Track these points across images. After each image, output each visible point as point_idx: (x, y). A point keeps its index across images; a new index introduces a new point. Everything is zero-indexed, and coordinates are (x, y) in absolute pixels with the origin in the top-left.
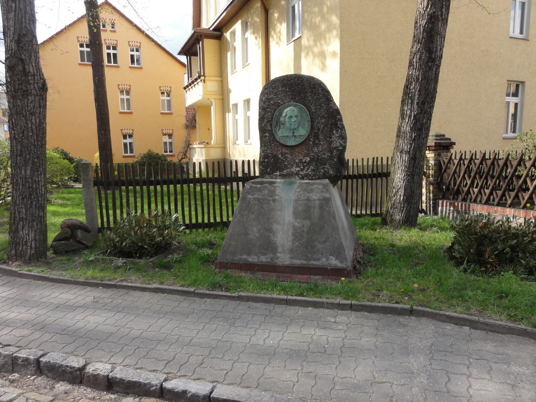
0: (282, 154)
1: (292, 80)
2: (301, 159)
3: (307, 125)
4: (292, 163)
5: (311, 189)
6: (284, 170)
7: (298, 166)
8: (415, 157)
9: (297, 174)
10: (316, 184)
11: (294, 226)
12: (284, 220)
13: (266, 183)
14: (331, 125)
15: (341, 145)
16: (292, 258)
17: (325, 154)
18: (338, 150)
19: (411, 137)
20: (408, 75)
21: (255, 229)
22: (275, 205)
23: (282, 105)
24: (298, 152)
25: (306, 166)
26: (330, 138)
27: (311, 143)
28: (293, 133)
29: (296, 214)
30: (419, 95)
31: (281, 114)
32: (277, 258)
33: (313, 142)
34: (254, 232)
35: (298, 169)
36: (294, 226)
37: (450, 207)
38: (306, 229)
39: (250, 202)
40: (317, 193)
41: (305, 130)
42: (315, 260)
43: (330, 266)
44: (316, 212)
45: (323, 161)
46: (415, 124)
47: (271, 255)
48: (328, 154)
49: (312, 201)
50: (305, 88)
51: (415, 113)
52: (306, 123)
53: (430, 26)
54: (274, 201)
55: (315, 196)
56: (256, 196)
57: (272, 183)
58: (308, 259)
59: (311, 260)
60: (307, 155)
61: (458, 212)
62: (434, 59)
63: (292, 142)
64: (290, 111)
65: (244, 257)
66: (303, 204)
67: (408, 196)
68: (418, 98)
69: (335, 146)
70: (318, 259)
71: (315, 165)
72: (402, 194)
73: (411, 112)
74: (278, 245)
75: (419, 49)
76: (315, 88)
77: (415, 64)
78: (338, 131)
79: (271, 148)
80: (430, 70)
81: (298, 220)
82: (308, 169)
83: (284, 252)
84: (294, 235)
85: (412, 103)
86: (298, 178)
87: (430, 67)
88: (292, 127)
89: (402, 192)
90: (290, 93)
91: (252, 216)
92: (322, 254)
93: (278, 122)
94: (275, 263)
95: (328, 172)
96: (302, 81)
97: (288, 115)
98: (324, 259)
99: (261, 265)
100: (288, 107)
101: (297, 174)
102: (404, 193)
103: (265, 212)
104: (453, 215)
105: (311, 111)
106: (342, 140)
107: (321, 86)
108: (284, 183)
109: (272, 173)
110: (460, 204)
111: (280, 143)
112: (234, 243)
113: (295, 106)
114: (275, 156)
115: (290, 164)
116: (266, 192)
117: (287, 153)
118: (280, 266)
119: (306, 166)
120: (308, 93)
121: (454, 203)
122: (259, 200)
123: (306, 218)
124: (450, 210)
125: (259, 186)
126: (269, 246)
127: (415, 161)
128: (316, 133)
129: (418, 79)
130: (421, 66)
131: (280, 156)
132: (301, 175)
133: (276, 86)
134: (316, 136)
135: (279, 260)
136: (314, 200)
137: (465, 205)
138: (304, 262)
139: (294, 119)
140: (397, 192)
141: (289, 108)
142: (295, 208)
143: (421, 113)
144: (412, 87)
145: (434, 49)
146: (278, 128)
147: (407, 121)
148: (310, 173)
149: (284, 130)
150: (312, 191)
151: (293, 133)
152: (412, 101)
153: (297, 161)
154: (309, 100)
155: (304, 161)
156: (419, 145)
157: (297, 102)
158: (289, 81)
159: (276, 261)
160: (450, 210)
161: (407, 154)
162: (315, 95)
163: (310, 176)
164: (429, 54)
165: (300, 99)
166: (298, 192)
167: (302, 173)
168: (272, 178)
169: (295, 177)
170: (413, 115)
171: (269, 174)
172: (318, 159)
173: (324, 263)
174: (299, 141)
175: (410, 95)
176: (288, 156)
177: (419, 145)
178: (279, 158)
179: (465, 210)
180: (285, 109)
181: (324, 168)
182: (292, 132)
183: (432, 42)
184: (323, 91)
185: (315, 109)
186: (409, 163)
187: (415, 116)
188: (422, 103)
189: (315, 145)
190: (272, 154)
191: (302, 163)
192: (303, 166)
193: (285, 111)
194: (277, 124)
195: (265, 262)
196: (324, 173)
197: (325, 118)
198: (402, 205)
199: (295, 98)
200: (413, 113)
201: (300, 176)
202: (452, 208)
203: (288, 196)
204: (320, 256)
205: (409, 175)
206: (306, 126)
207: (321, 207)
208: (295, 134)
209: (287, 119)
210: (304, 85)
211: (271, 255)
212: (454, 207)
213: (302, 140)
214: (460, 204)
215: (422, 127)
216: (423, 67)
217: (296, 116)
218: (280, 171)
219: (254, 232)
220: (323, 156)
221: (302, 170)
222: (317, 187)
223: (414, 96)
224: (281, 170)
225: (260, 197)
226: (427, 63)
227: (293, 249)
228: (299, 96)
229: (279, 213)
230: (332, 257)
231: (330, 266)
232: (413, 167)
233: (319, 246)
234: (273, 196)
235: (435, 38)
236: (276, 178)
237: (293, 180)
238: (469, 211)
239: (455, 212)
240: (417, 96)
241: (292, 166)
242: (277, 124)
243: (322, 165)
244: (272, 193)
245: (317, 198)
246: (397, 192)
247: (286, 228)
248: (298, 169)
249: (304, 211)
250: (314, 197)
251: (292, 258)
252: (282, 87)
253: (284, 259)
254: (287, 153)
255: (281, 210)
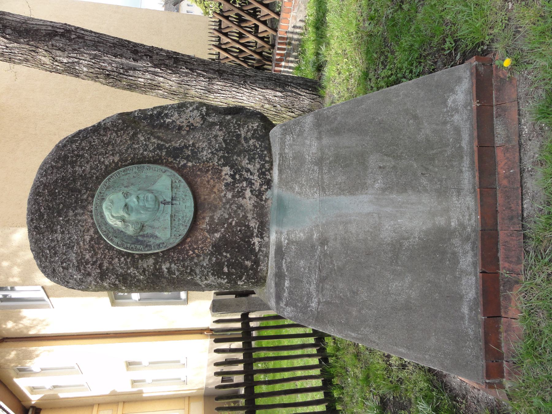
0: (212, 231)
1: (39, 210)
2: (227, 185)
3: (150, 171)
4: (234, 207)
5: (294, 158)
6: (248, 227)
7: (240, 194)
8: (218, 71)
9: (259, 195)
10: (282, 148)
11: (384, 190)
12: (369, 214)
13: (279, 267)
14: (154, 127)
15: (197, 108)
16: (459, 191)
17: (216, 136)
18: (208, 114)
19: (187, 74)
20: (88, 76)
21: (395, 285)
22: (335, 239)
23: (96, 232)
24: (209, 194)
25: (241, 175)
26: (180, 128)
27: (190, 164)
28: (165, 203)
29: (355, 187)
30: (122, 56)
31: (117, 233)
32: (463, 226)
33: (189, 161)
34: (402, 287)
35: (248, 193)
36: (384, 190)
37: (281, 66)
38: (390, 163)
39: (327, 303)
40: (304, 144)
41: (159, 177)
42: (458, 139)
43: (470, 104)
44: (349, 142)
45: (231, 140)
46: (167, 66)
47: (456, 241)
48: (216, 130)
49: (323, 153)
50: (63, 179)
51: (150, 65)
52: (143, 175)
53: (9, 31)
54: (324, 242)
55: (311, 147)
56: (313, 287)
57: (280, 252)
58: (459, 154)
59: (460, 147)
60: (217, 172)
61: (288, 55)
62: (66, 30)
63: (187, 207)
64: (114, 211)
65: (465, 310)
66: (329, 172)
67: (275, 84)
68: (126, 58)
69: (198, 119)
70: (457, 130)
71: (239, 155)
72: (273, 92)
73: (148, 72)
74: (429, 225)
75: (46, 51)
76: (66, 157)
77: (71, 60)
78: (166, 115)
79: (198, 256)
80: (83, 38)
81: (369, 182)
82: (248, 170)
83: (447, 210)
84: (403, 189)
85: (135, 69)
86: (269, 193)
87: (79, 37)
88: (150, 204)
89: (270, 94)
90: (71, 213)
91: (363, 295)
92: (445, 123)
93: (136, 240)
94: (474, 231)
95: (255, 130)
96: (45, 186)
97: (122, 213)
98: (456, 117)
99: (483, 266)
100: (103, 217)
101: (259, 195)
102: (272, 89)
103: (351, 262)
104: (292, 62)
105: (117, 164)
106: (187, 108)
107: (65, 146)
108: (280, 223)
109: (256, 255)
110: (278, 52)
111: (188, 235)
112: (433, 340)
113: (103, 199)
114: (217, 248)
115: (235, 212)
116: (302, 263)
117: (212, 218)
118: (482, 217)
119: (241, 175)
120: (75, 172)
121: (277, 60)
122: (322, 280)
123: (363, 163)
124: (285, 67)
125: (287, 283)
126: (435, 248)
127: (224, 72)
128: (169, 153)
129: (95, 57)
130: (75, 50)
131: (217, 235)
132: (261, 185)
133: (49, 248)
134: (176, 153)
135: (466, 222)
136: (321, 149)
137: (279, 43)
138: (466, 162)
139: (133, 201)
140: (269, 102)
141: (107, 214)
142: (342, 191)
143: (151, 57)
144: (109, 68)
145: (50, 28)
146: (152, 240)
147: (161, 79)
148: (258, 166)
149: (156, 224)
150: (299, 157)
151: (165, 203)
152: (130, 69)
153: (229, 195)
154: (91, 168)
155: (230, 180)
156: (199, 65)
157: (93, 197)
158: (41, 216)
159: (469, 229)
160: (285, 67)
161: (214, 82)
162: (82, 156)
163: (263, 166)
164: (55, 36)
165: (87, 189)
166: (301, 186)
167: (257, 186)
168: (267, 255)
169: (266, 200)
170: (153, 69)
171: (257, 262)
172: (227, 150)
173: (465, 117)
174: (184, 190)
175: (122, 71)
176: (217, 215)
177: (199, 65)
178: (223, 238)
179: (286, 44)
180: (106, 223)
181: (246, 139)
182: (162, 206)
183: (37, 30)
184: (76, 141)
185: (113, 155)
186: (227, 80)
187: (155, 66)
188: (135, 54)
189: (194, 155)
190: (212, 254)
191: (234, 183)
192: (240, 181)
193: (111, 221)
194: (142, 243)
195: (475, 255)
196: (258, 139)
197: (135, 134)
198: (289, 94)
199: (82, 201)
200: (150, 69)
201: (265, 187)
202: (283, 64)
203: (307, 211)
204: (448, 126)
205: (245, 82)
206: (150, 173)
207: (337, 132)
208: (170, 200)
209: (133, 217)
210: (56, 181)
211: (456, 241)
212: (281, 60)
213: (184, 183)
214: (278, 52)
215: (172, 57)
216: (76, 47)
217: (126, 195)
218: (252, 236)
219: (402, 287)
220: (220, 139)
221: (250, 183)
222: (291, 145)
223: (122, 64)
224: (248, 235)
225: (314, 277)
226: (70, 40)
227: (438, 191)
228: (80, 191)
229: (353, 228)
230: (450, 102)
231: (470, 104)
232: (232, 75)
233: (427, 130)
234: (313, 246)
235: (32, 26)
236: (267, 245)
237: (272, 205)
238: (287, 38)
239: (288, 59)
240: (124, 60)
241: (240, 206)
242: (142, 243)
243: (239, 142)
244: (305, 248)
245: (315, 144)
246: (269, 102)
247: (389, 209)
248: (248, 193)
249: (346, 171)
250: (314, 149)
251: (459, 191)
252: (53, 231)
253: (463, 210)
254: (212, 218)
255: (345, 223)
